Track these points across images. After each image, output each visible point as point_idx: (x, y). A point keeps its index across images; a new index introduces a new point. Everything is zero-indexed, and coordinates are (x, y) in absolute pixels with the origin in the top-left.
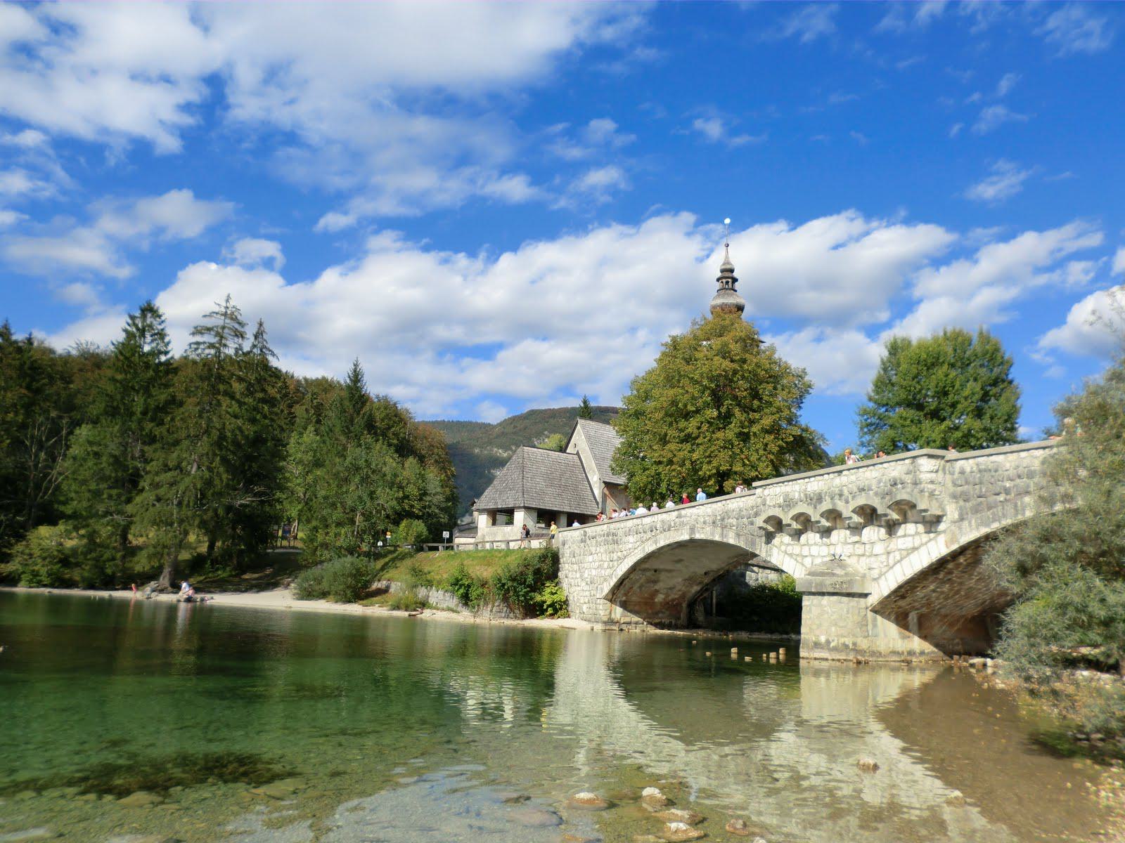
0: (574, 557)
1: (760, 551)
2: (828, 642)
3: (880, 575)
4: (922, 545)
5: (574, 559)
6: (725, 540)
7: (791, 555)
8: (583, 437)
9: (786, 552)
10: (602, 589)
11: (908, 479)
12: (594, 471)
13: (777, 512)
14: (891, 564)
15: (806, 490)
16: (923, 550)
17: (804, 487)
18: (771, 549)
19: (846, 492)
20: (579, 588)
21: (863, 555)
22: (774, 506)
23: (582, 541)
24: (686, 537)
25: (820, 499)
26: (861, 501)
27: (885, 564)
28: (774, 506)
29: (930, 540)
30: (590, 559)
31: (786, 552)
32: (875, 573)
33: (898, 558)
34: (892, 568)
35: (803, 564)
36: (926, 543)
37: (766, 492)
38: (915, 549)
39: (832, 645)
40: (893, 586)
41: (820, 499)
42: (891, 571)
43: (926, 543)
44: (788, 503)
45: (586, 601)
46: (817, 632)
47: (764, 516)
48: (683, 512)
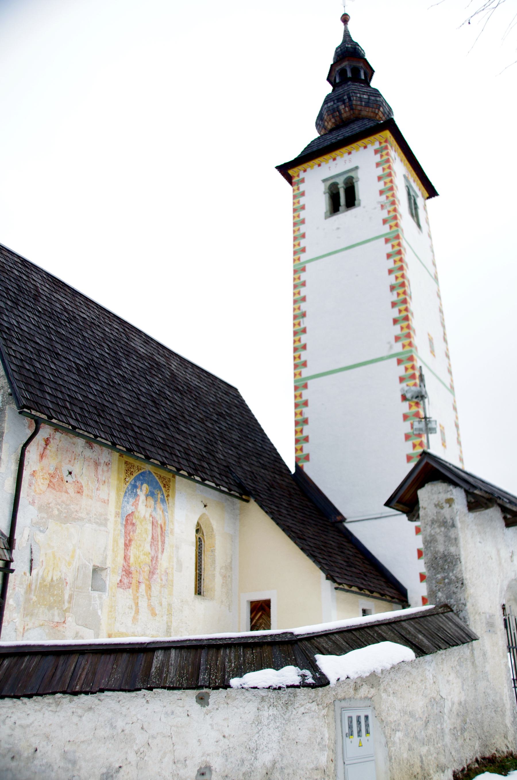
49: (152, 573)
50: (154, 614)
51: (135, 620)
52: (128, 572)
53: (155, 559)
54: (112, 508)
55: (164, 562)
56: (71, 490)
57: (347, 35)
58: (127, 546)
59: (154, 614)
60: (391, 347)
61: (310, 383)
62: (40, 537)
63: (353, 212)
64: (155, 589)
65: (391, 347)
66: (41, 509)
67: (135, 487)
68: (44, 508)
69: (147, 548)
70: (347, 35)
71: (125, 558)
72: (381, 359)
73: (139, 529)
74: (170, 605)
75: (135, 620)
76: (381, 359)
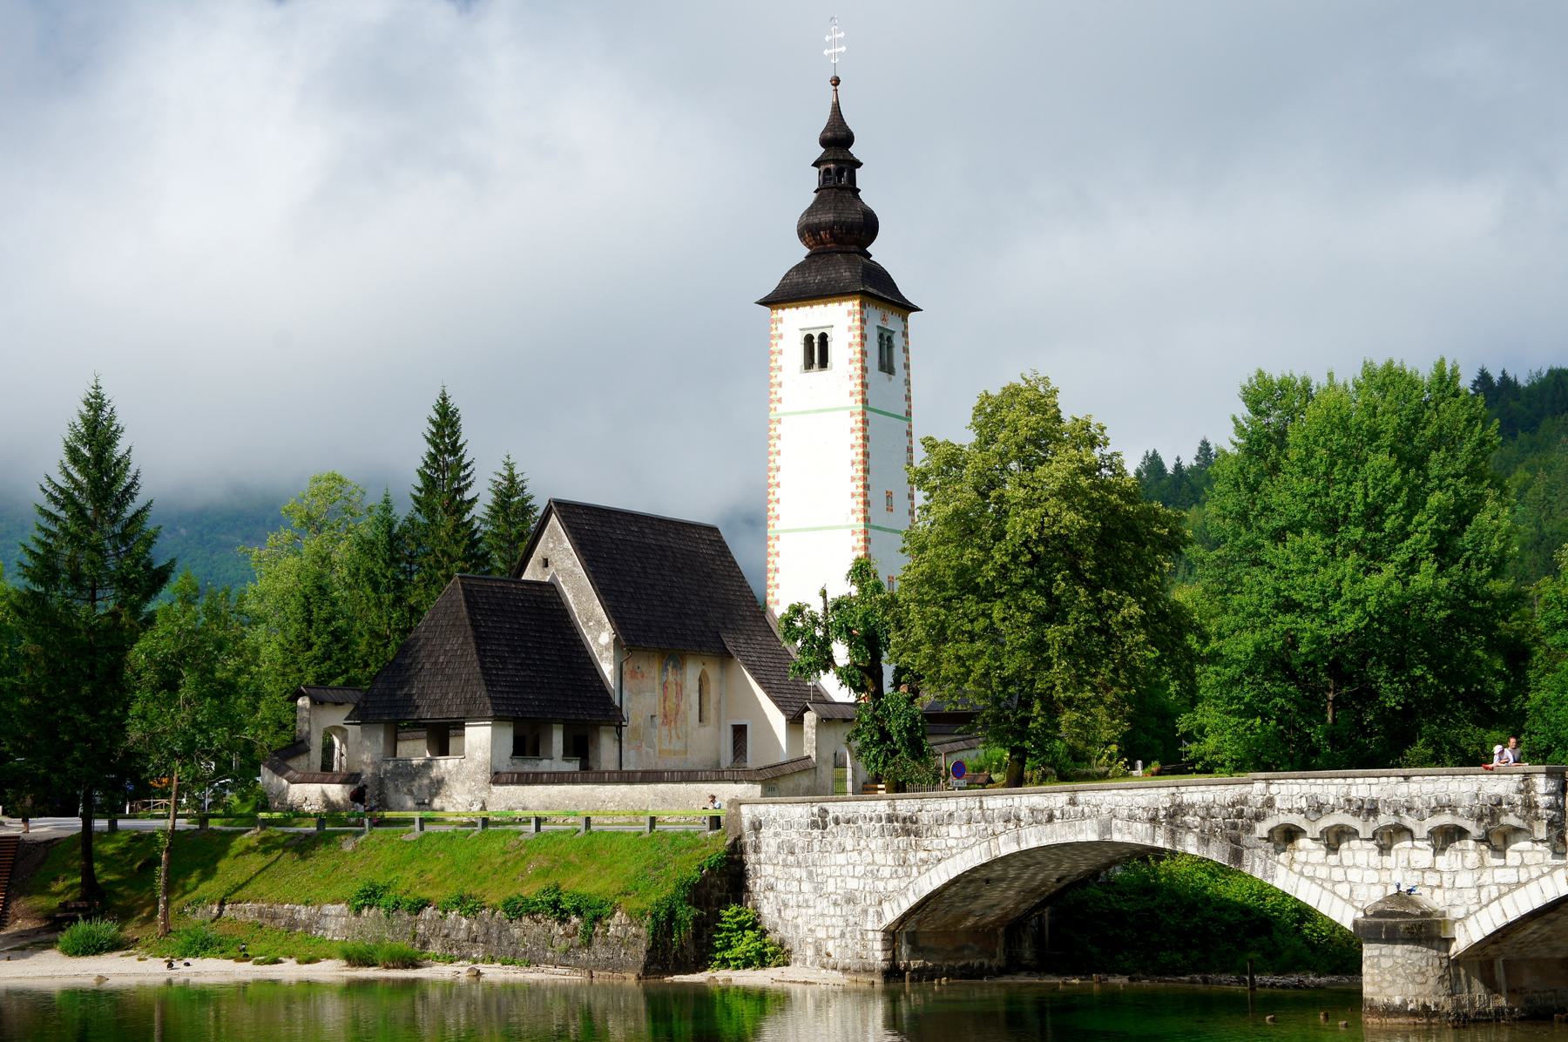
0: (792, 853)
1: (1253, 867)
2: (1405, 1003)
3: (1468, 915)
4: (1530, 880)
5: (791, 858)
6: (1156, 845)
7: (1312, 879)
8: (568, 544)
9: (1302, 874)
10: (880, 915)
11: (1518, 799)
12: (599, 622)
13: (1296, 820)
14: (1484, 902)
15: (1348, 794)
16: (1533, 886)
17: (1345, 790)
18: (1273, 867)
19: (1418, 803)
20: (811, 911)
21: (1439, 887)
22: (1290, 811)
23: (814, 825)
24: (1093, 837)
25: (1373, 811)
26: (1446, 819)
27: (1476, 900)
28: (1290, 811)
29: (1543, 875)
30: (841, 858)
31: (1302, 874)
32: (1457, 913)
33: (1495, 894)
34: (1487, 906)
35: (1334, 893)
36: (1538, 878)
37: (1274, 789)
38: (1519, 884)
39: (1410, 1007)
40: (1489, 930)
41: (1373, 811)
42: (1485, 910)
43: (1538, 878)
44: (1319, 809)
45: (837, 933)
46: (1389, 991)
47: (1270, 823)
48: (1081, 797)
49: (677, 714)
50: (679, 738)
51: (670, 742)
52: (665, 716)
53: (678, 705)
54: (657, 681)
55: (682, 707)
56: (639, 676)
57: (836, 109)
58: (665, 701)
59: (679, 738)
60: (848, 519)
61: (782, 536)
62: (630, 705)
63: (824, 373)
64: (679, 723)
65: (848, 519)
66: (629, 691)
67: (666, 665)
68: (630, 691)
69: (674, 700)
70: (836, 109)
71: (664, 708)
72: (840, 527)
73: (669, 689)
74: (686, 732)
75: (670, 742)
76: (840, 527)
